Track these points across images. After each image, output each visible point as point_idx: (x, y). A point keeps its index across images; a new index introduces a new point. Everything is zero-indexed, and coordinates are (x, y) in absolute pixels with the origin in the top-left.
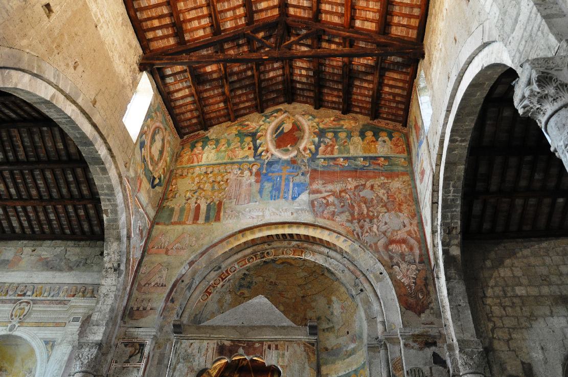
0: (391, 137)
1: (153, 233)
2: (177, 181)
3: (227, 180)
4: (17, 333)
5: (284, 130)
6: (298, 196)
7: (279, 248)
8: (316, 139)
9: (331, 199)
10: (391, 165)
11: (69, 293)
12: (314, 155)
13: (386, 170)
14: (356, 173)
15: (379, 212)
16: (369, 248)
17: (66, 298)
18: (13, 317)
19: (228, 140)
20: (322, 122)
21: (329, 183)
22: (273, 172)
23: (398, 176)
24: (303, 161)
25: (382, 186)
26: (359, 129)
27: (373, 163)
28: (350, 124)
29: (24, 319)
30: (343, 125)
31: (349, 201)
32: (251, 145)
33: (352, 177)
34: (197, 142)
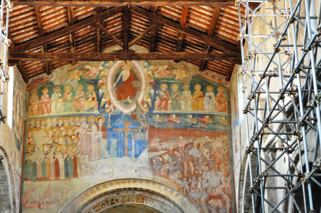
0: (216, 92)
1: (25, 189)
2: (32, 134)
3: (78, 134)
5: (123, 78)
6: (140, 154)
7: (126, 196)
8: (152, 91)
9: (166, 157)
10: (214, 124)
12: (150, 114)
13: (210, 129)
14: (186, 132)
15: (203, 171)
16: (194, 203)
19: (73, 88)
20: (157, 70)
21: (165, 140)
22: (117, 127)
23: (219, 136)
24: (142, 116)
25: (207, 145)
26: (189, 81)
27: (200, 120)
28: (181, 74)
30: (175, 75)
31: (180, 159)
32: (94, 95)
33: (183, 136)
34: (42, 88)
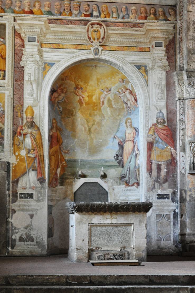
4: (104, 56)
11: (140, 14)
17: (139, 21)
18: (92, 40)
29: (105, 43)
